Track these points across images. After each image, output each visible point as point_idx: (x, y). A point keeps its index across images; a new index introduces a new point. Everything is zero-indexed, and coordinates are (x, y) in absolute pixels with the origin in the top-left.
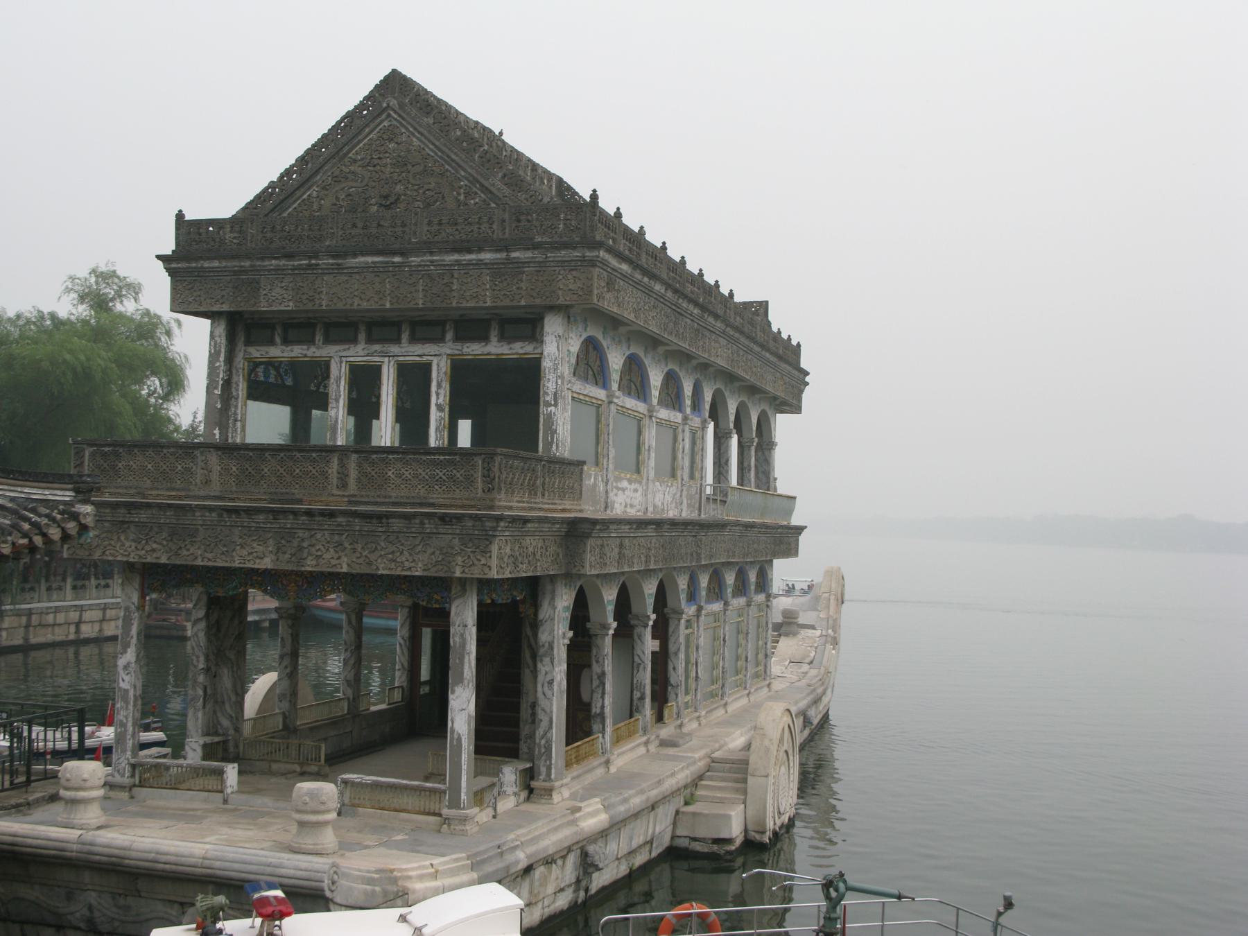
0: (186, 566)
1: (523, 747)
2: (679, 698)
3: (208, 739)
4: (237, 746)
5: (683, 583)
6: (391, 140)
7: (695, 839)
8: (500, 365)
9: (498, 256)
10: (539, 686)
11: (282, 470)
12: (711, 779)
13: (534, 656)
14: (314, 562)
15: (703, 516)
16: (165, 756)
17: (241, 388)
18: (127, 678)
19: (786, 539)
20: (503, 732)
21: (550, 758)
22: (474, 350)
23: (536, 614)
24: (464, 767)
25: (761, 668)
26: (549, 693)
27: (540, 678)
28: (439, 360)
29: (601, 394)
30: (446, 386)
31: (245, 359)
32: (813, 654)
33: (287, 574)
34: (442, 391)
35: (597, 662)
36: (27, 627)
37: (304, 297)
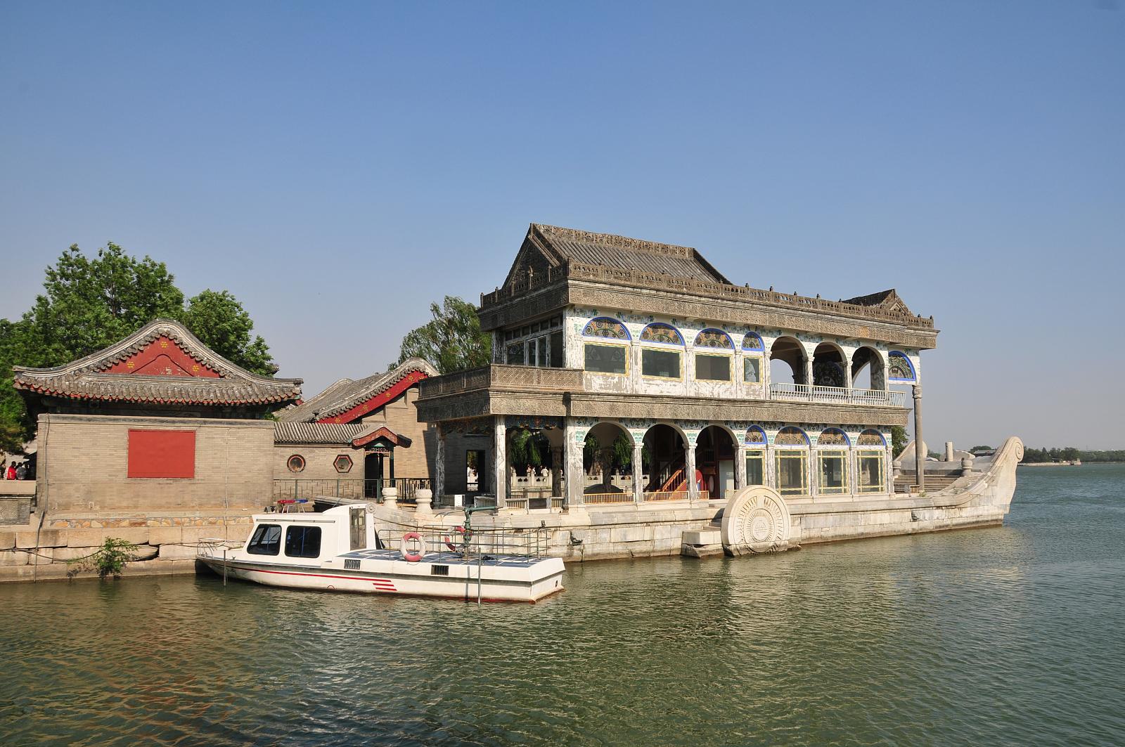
5: (739, 434)
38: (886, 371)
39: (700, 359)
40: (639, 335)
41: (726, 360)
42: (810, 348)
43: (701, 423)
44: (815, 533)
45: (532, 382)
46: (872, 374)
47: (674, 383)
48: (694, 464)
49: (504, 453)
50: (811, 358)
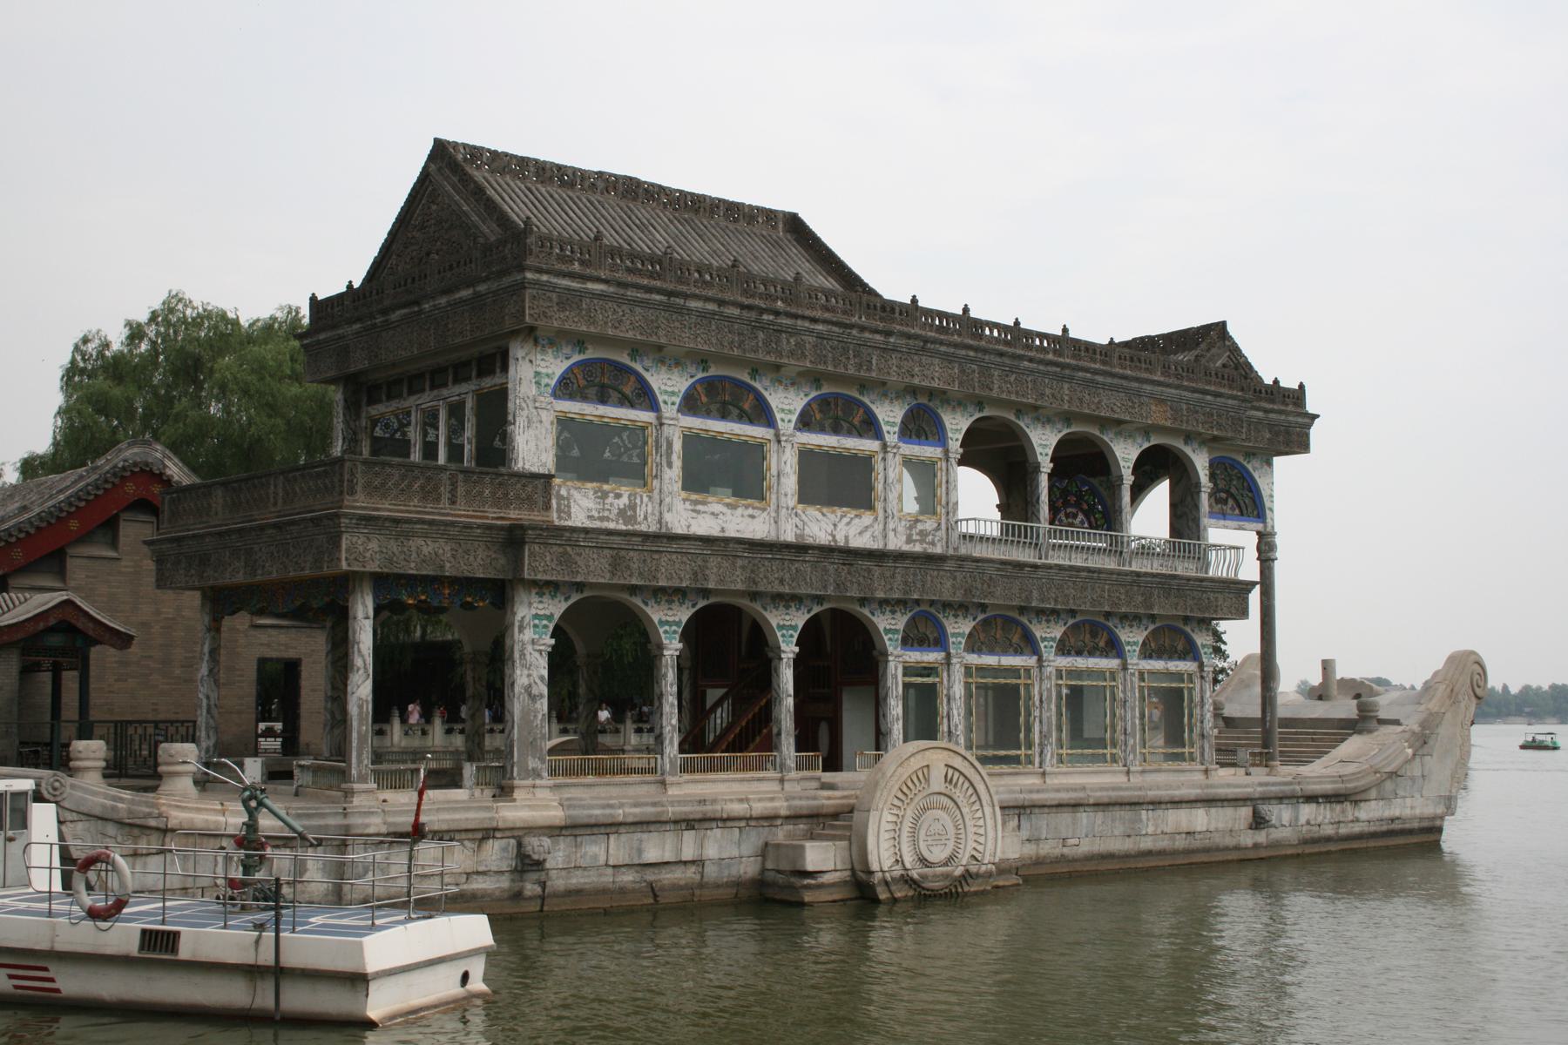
5: (888, 625)
7: (779, 872)
38: (1204, 498)
39: (807, 457)
40: (678, 400)
41: (864, 464)
42: (1043, 442)
43: (809, 603)
44: (1049, 848)
45: (438, 500)
46: (1173, 506)
47: (750, 511)
48: (791, 691)
49: (370, 660)
50: (1046, 466)
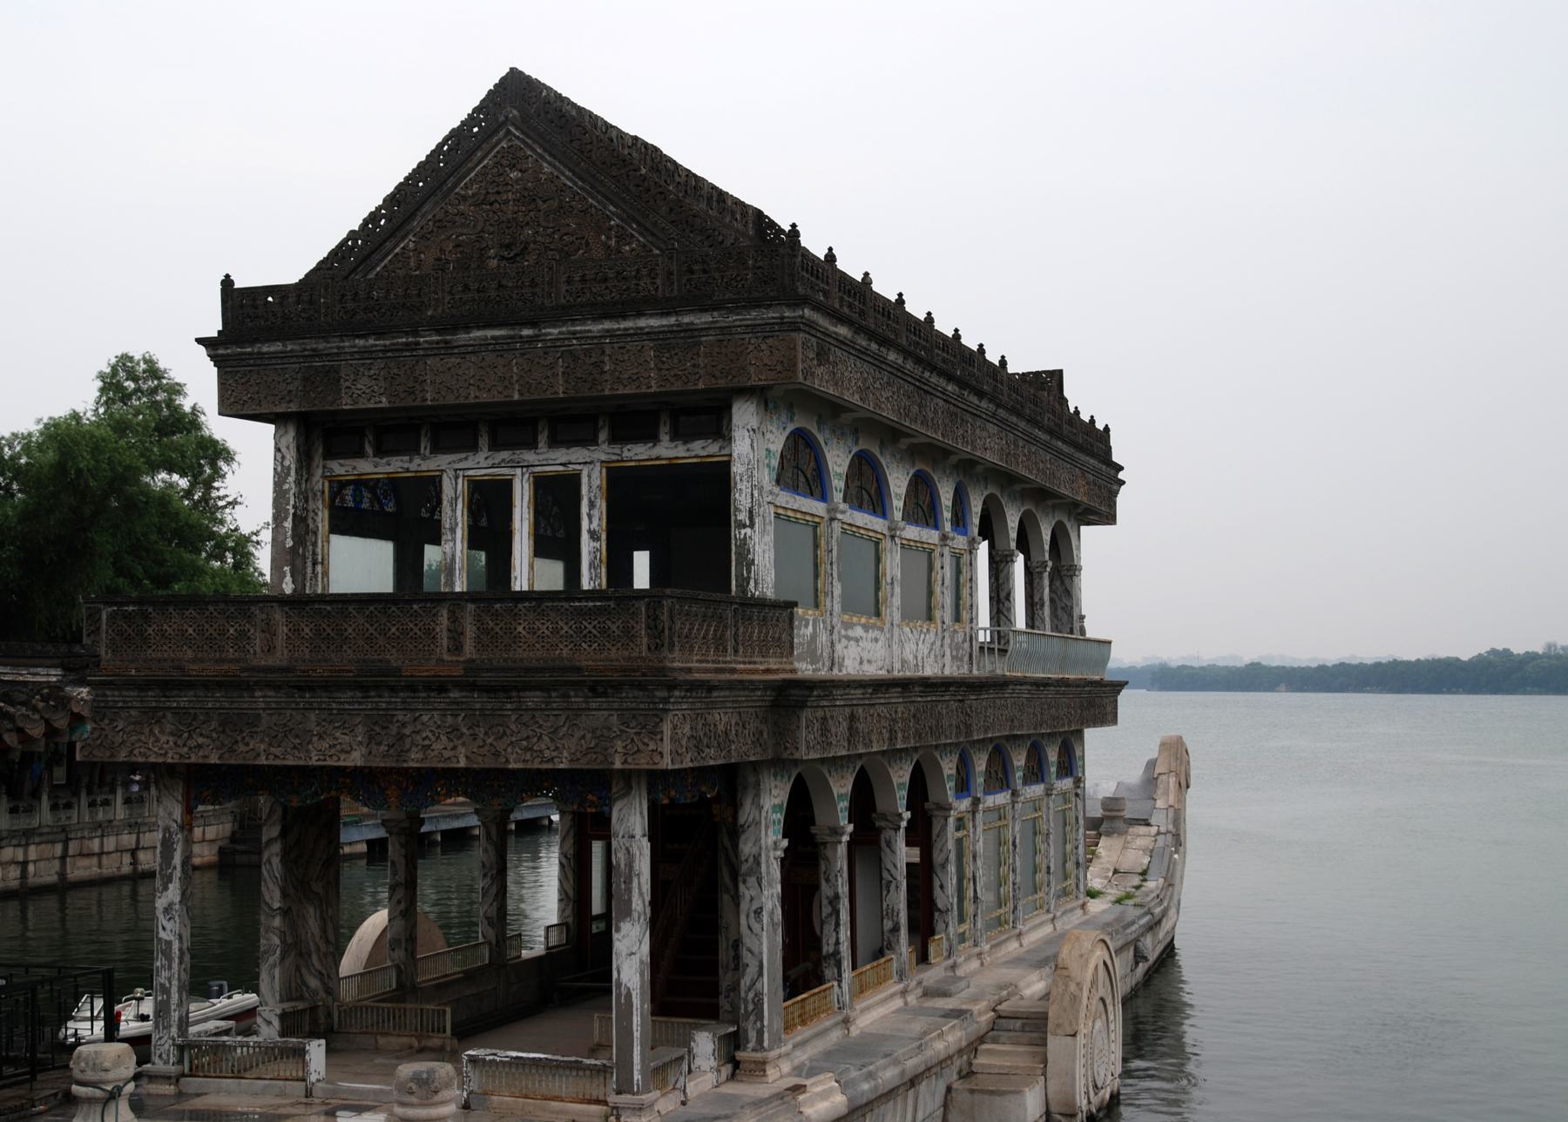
0: (247, 766)
1: (724, 1003)
2: (951, 929)
3: (287, 1006)
4: (329, 1015)
5: (949, 767)
6: (512, 167)
8: (672, 473)
9: (665, 322)
10: (743, 921)
11: (371, 630)
12: (995, 1041)
13: (735, 875)
14: (420, 756)
15: (975, 672)
16: (227, 1032)
17: (322, 519)
18: (168, 926)
19: (1097, 699)
20: (694, 983)
21: (760, 1017)
22: (638, 453)
23: (735, 816)
24: (637, 1034)
25: (1071, 881)
26: (756, 927)
27: (744, 906)
28: (590, 469)
29: (818, 508)
30: (602, 505)
31: (324, 477)
32: (1146, 860)
33: (387, 772)
34: (596, 513)
35: (828, 880)
36: (63, 858)
37: (401, 389)
